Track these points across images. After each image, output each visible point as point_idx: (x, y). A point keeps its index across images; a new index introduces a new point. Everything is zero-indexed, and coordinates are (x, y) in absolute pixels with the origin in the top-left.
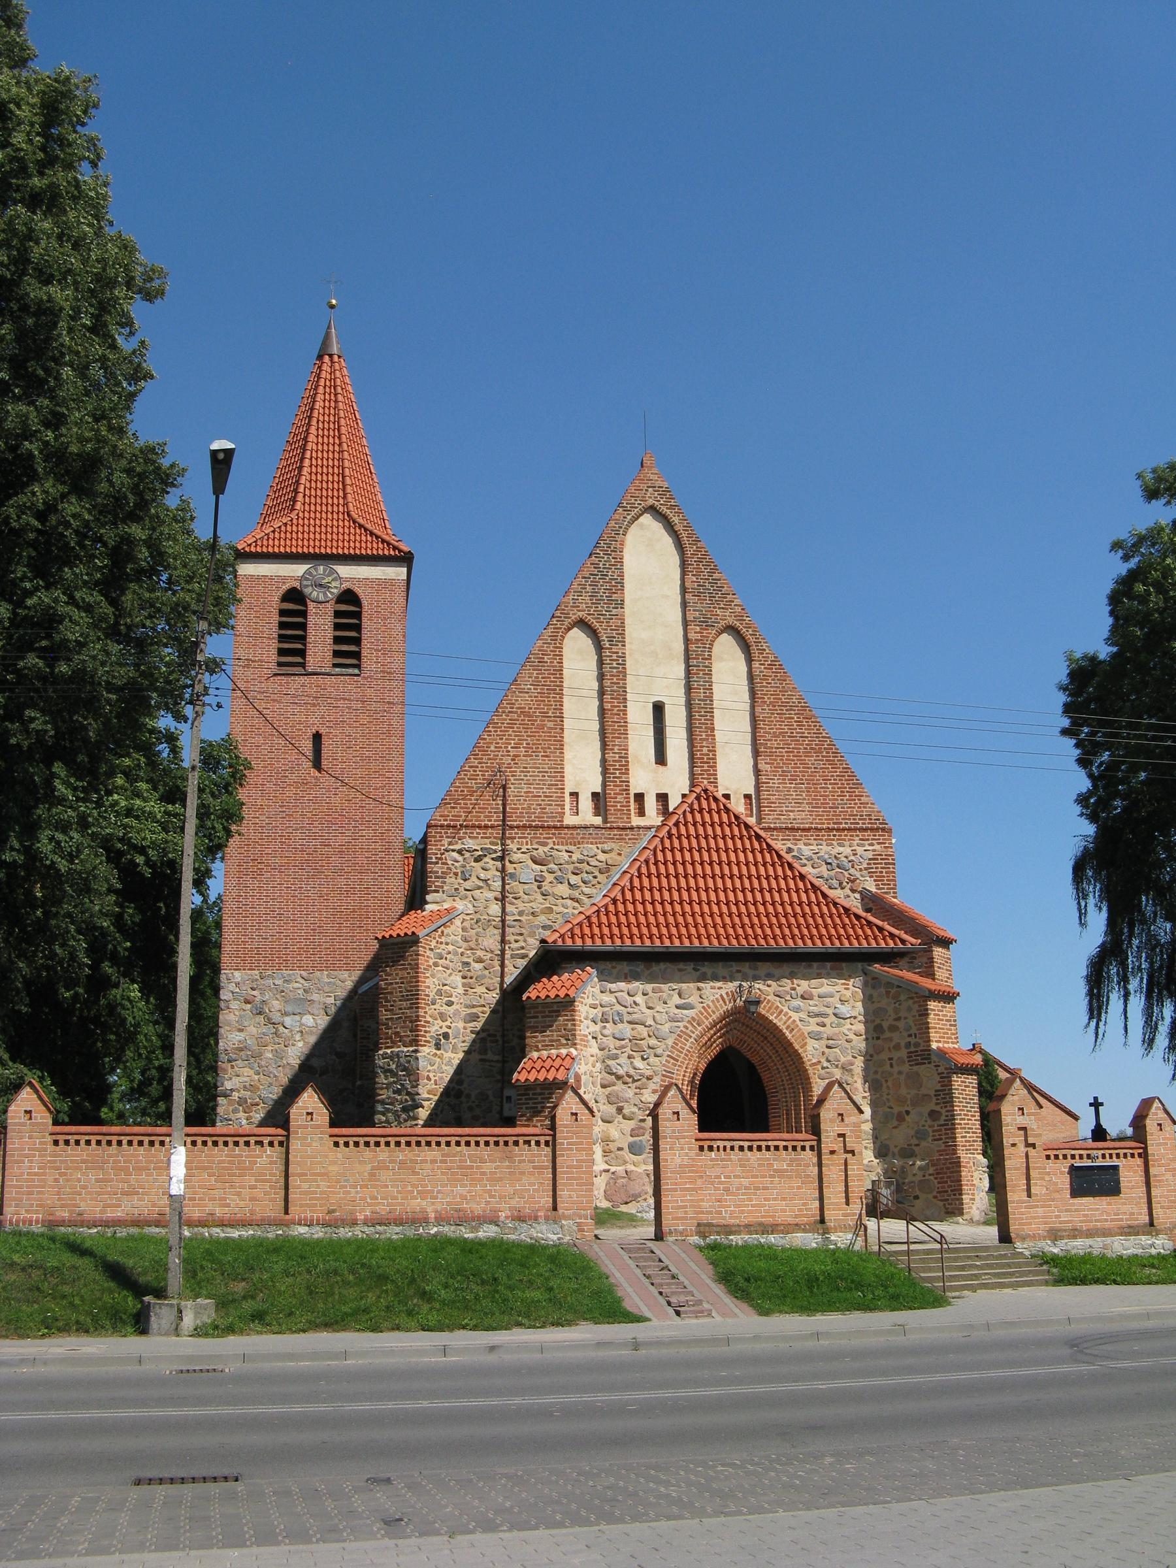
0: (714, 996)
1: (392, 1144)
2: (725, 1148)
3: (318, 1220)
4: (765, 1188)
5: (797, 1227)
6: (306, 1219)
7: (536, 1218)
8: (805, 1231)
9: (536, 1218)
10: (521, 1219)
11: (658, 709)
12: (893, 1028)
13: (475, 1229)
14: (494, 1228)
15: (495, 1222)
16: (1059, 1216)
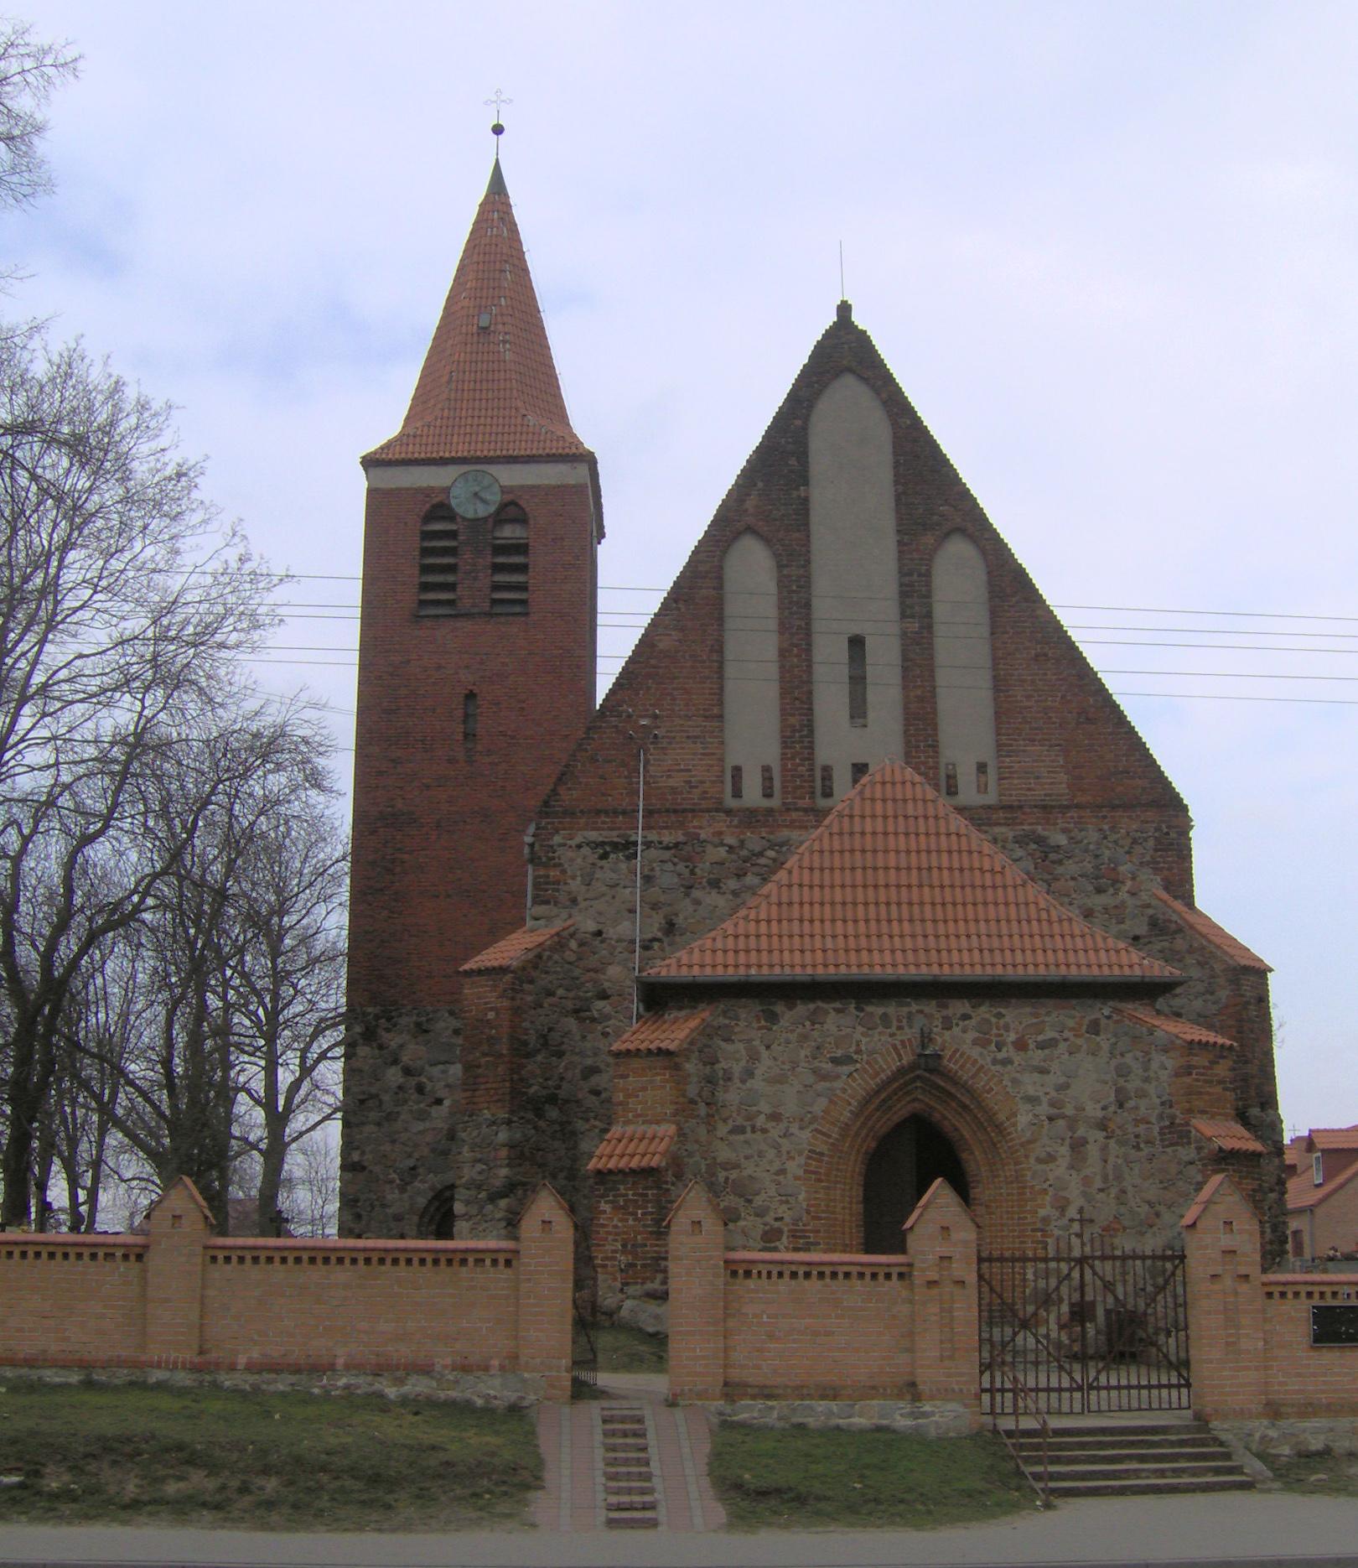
0: (881, 1043)
1: (291, 1260)
2: (769, 1273)
3: (183, 1363)
4: (828, 1334)
5: (872, 1391)
6: (167, 1362)
7: (486, 1369)
8: (885, 1396)
9: (486, 1369)
10: (465, 1369)
11: (857, 644)
12: (1141, 1094)
13: (400, 1382)
14: (424, 1380)
15: (426, 1370)
16: (1285, 1384)
